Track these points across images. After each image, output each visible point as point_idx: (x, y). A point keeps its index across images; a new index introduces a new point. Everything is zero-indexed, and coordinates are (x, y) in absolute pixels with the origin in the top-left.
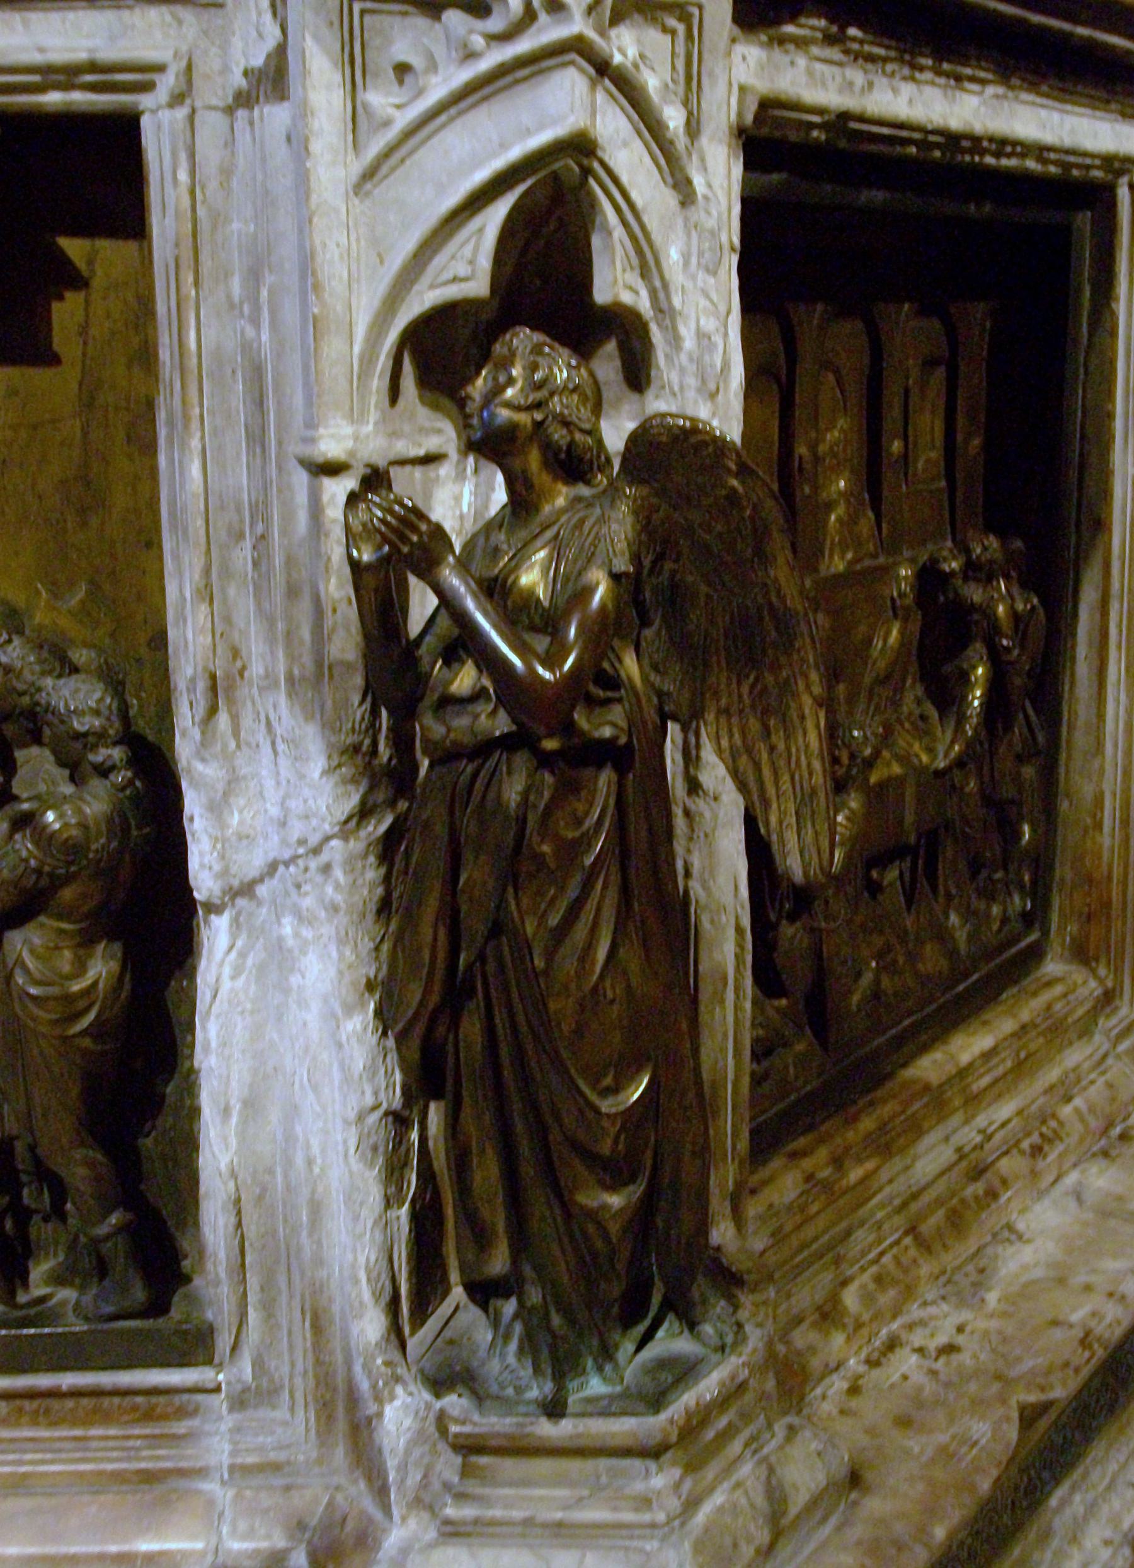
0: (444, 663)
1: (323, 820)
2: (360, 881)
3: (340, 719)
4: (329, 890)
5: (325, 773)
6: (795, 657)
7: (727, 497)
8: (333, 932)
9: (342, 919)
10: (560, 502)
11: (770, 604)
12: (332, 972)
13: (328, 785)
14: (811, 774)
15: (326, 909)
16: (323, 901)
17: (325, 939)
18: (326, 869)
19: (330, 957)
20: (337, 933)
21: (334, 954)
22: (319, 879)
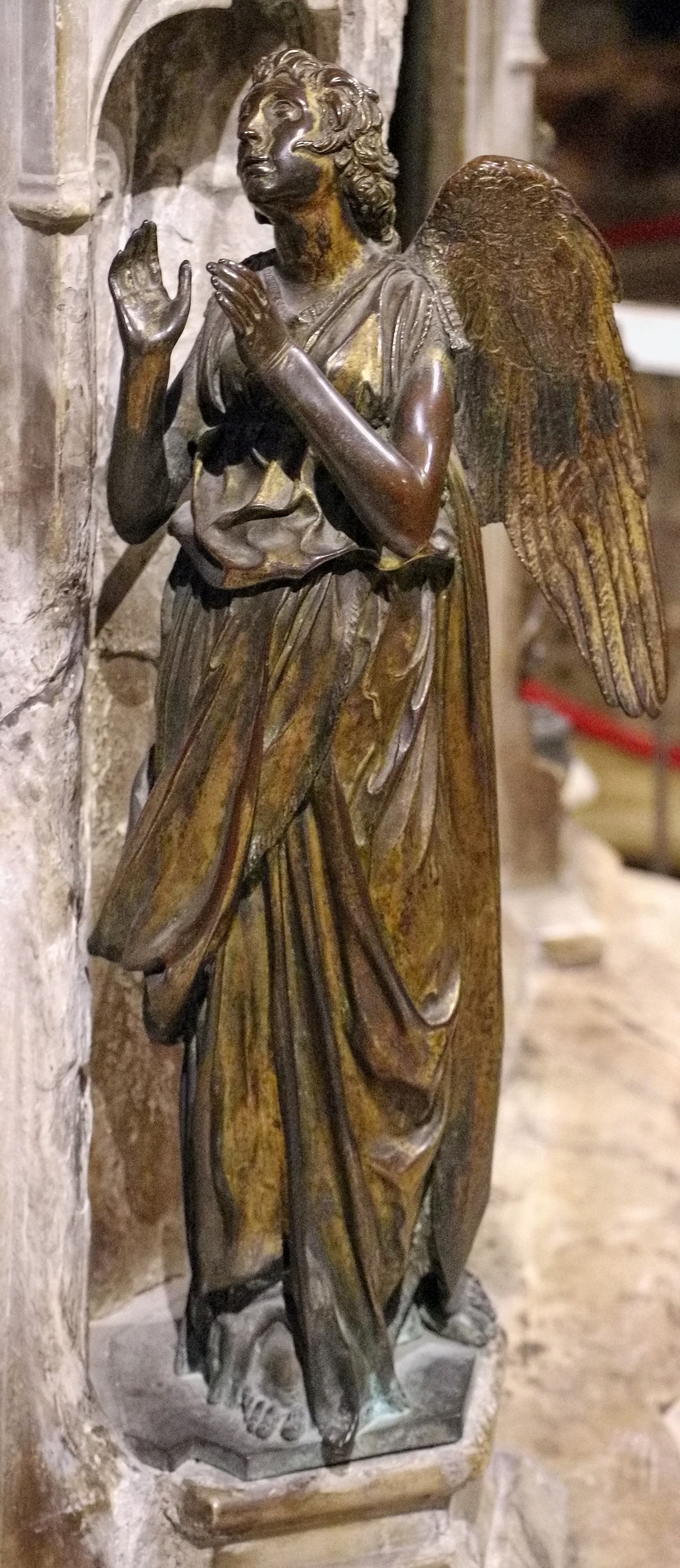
0: (206, 466)
1: (26, 678)
2: (61, 757)
3: (68, 544)
4: (26, 771)
5: (33, 614)
6: (614, 441)
7: (555, 255)
8: (31, 826)
9: (43, 808)
10: (358, 265)
11: (588, 377)
12: (26, 883)
13: (33, 631)
14: (638, 584)
15: (20, 797)
16: (15, 786)
17: (17, 838)
18: (24, 743)
19: (24, 861)
20: (37, 829)
21: (31, 857)
22: (13, 756)
